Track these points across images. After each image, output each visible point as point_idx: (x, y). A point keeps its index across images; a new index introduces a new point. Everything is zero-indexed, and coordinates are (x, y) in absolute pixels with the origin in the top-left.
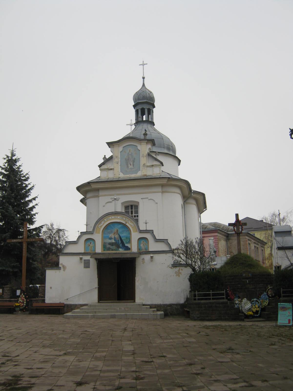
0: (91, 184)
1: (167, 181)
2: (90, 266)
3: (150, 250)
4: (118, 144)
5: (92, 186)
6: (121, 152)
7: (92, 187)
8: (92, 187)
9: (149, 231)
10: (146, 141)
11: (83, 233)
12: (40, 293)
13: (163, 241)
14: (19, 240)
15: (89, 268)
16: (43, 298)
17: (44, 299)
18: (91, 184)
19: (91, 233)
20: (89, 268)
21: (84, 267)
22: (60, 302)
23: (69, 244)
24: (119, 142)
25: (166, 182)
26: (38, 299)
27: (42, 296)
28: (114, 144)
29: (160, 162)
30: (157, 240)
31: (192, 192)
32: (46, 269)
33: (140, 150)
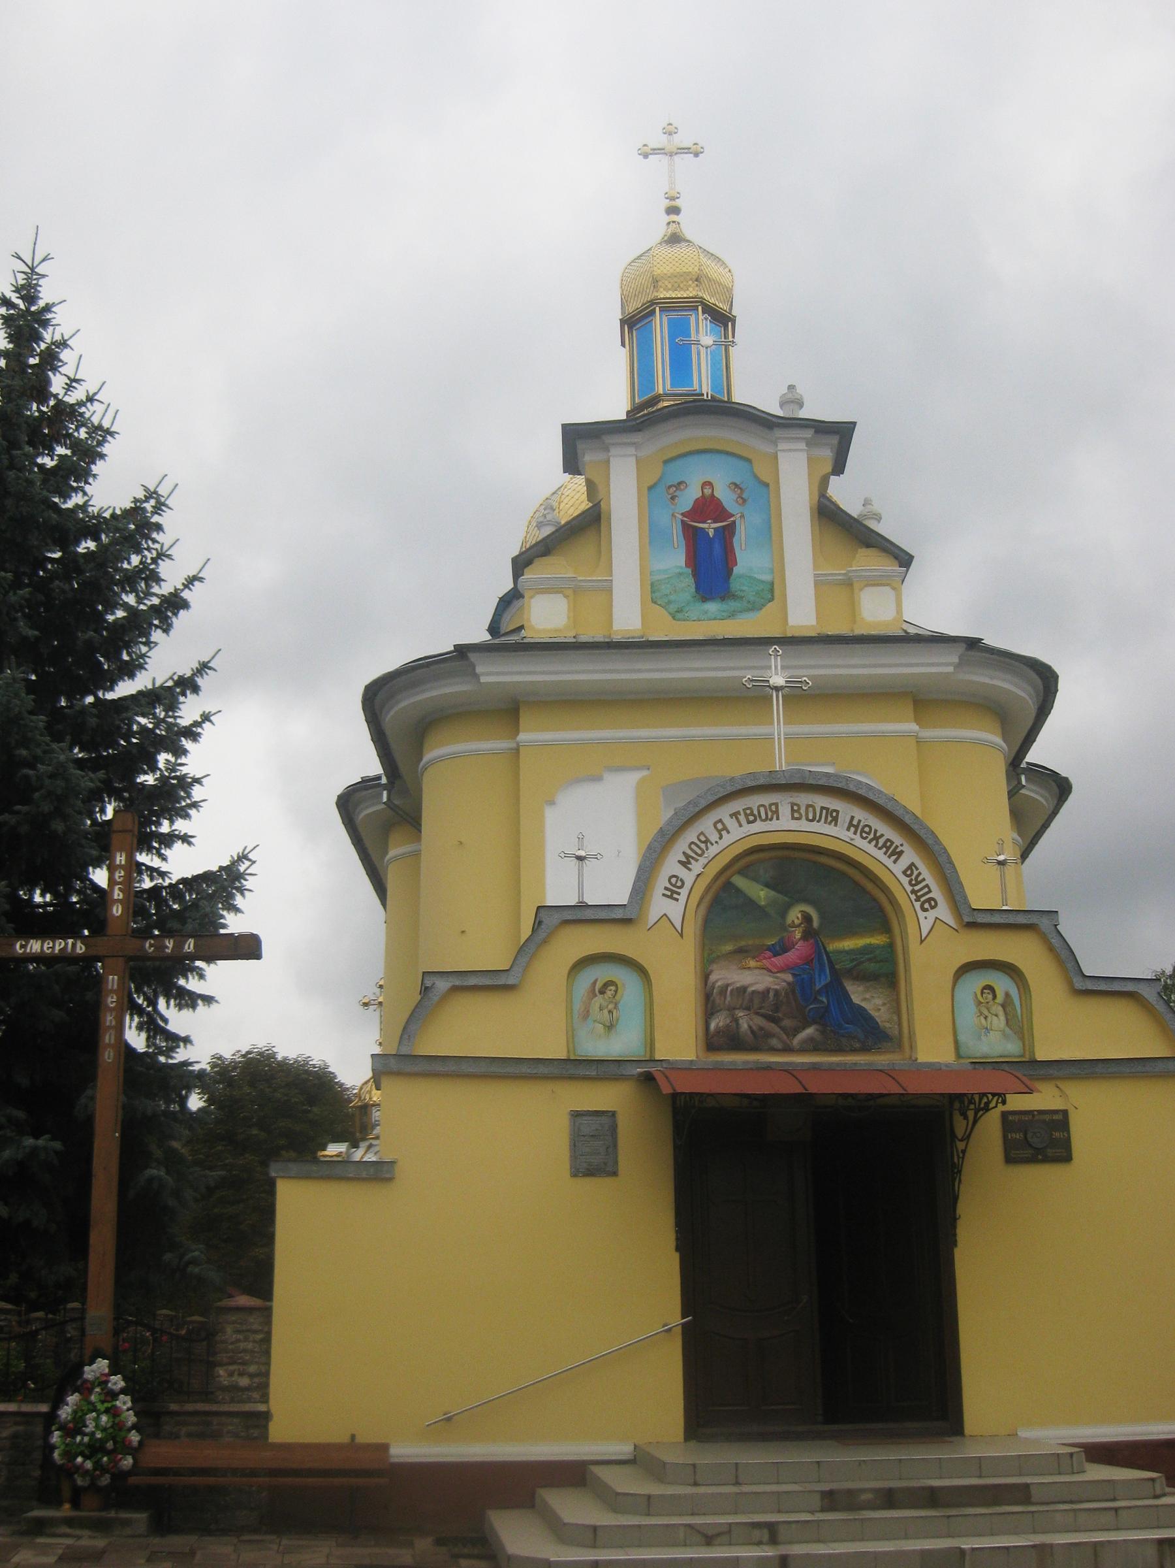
0: (473, 657)
1: (956, 660)
2: (616, 1163)
3: (1041, 1056)
4: (637, 438)
5: (479, 670)
6: (650, 488)
7: (476, 676)
8: (483, 679)
9: (1033, 919)
10: (809, 433)
11: (557, 918)
12: (221, 1365)
13: (1130, 987)
14: (70, 941)
15: (615, 1174)
16: (250, 1400)
17: (262, 1408)
18: (473, 657)
19: (619, 914)
20: (615, 1174)
21: (575, 1174)
22: (353, 1437)
23: (455, 989)
24: (640, 430)
25: (951, 669)
26: (214, 1408)
27: (244, 1382)
28: (608, 439)
29: (896, 558)
30: (1090, 986)
31: (1023, 765)
32: (273, 1174)
33: (767, 485)
